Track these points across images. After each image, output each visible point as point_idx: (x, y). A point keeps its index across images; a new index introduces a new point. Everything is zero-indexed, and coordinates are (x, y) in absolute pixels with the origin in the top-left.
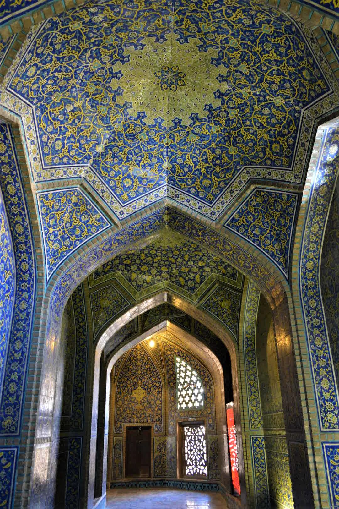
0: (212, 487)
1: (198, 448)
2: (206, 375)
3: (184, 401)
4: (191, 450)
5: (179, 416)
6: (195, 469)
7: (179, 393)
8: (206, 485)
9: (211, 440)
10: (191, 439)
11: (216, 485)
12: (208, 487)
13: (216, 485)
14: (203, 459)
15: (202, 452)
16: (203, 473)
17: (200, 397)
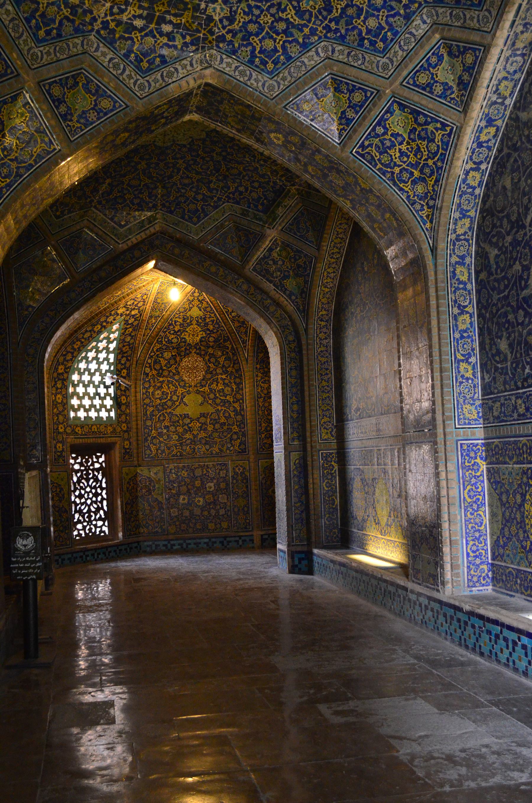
0: (131, 548)
1: (94, 491)
2: (128, 365)
3: (81, 406)
4: (81, 496)
5: (74, 432)
6: (88, 527)
7: (71, 390)
8: (123, 548)
9: (127, 474)
10: (81, 476)
11: (136, 544)
12: (126, 549)
13: (136, 544)
14: (102, 508)
15: (99, 498)
16: (101, 532)
17: (108, 402)
